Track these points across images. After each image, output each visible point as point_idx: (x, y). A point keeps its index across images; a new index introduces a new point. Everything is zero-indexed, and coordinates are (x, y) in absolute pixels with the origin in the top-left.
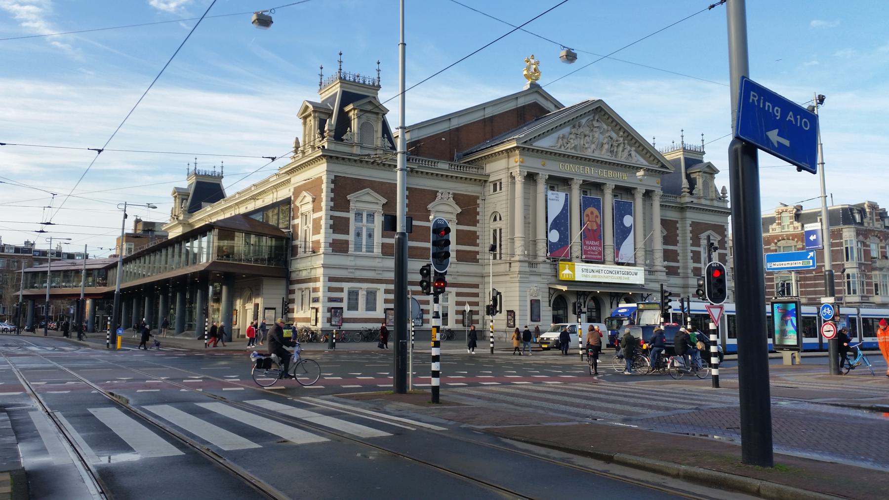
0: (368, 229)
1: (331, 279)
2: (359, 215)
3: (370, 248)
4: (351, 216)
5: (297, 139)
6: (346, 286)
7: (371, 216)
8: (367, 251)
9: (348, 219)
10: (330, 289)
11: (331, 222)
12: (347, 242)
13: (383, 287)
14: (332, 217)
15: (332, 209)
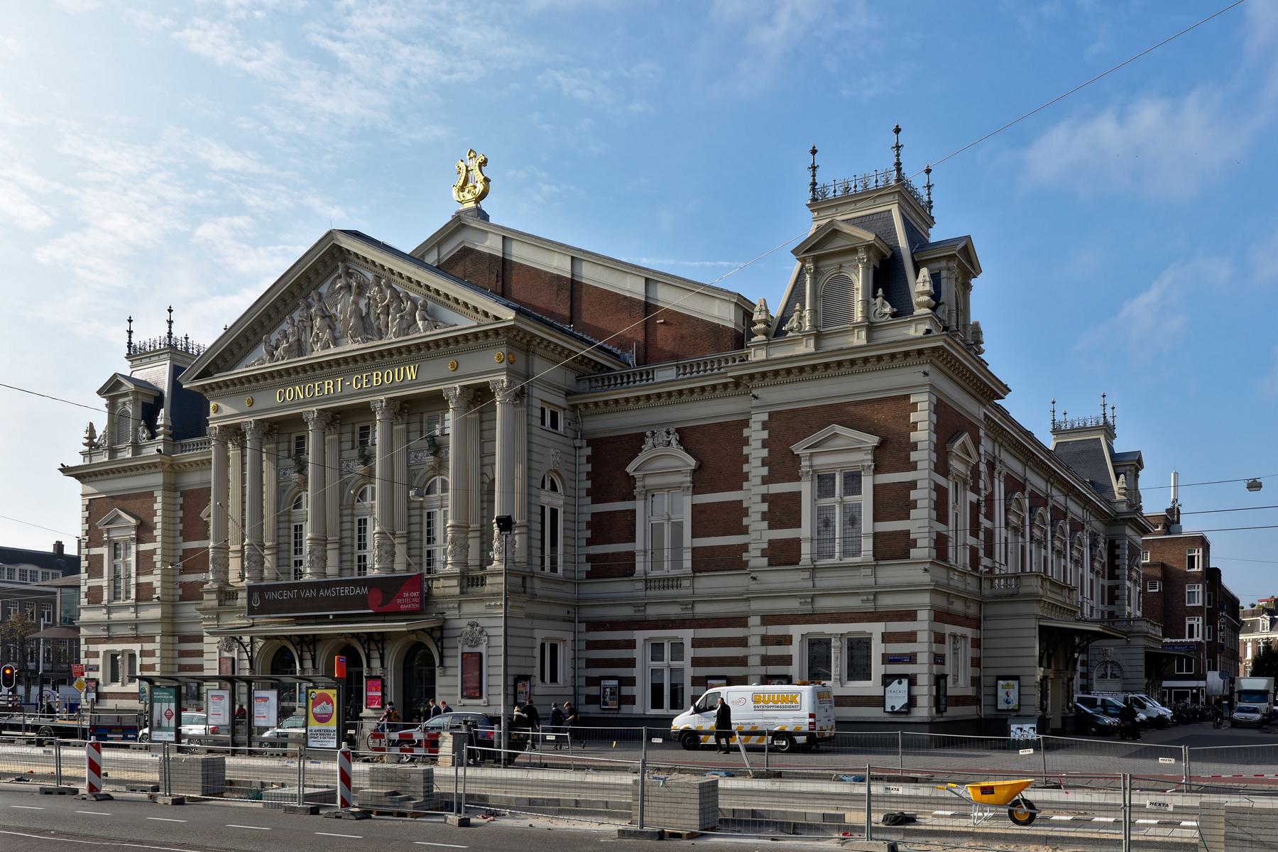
0: (845, 507)
1: (768, 619)
2: (824, 483)
3: (852, 547)
4: (806, 488)
5: (91, 430)
6: (796, 631)
7: (853, 483)
8: (845, 553)
9: (796, 496)
10: (766, 640)
11: (765, 507)
12: (797, 542)
13: (876, 629)
14: (765, 498)
15: (766, 481)
